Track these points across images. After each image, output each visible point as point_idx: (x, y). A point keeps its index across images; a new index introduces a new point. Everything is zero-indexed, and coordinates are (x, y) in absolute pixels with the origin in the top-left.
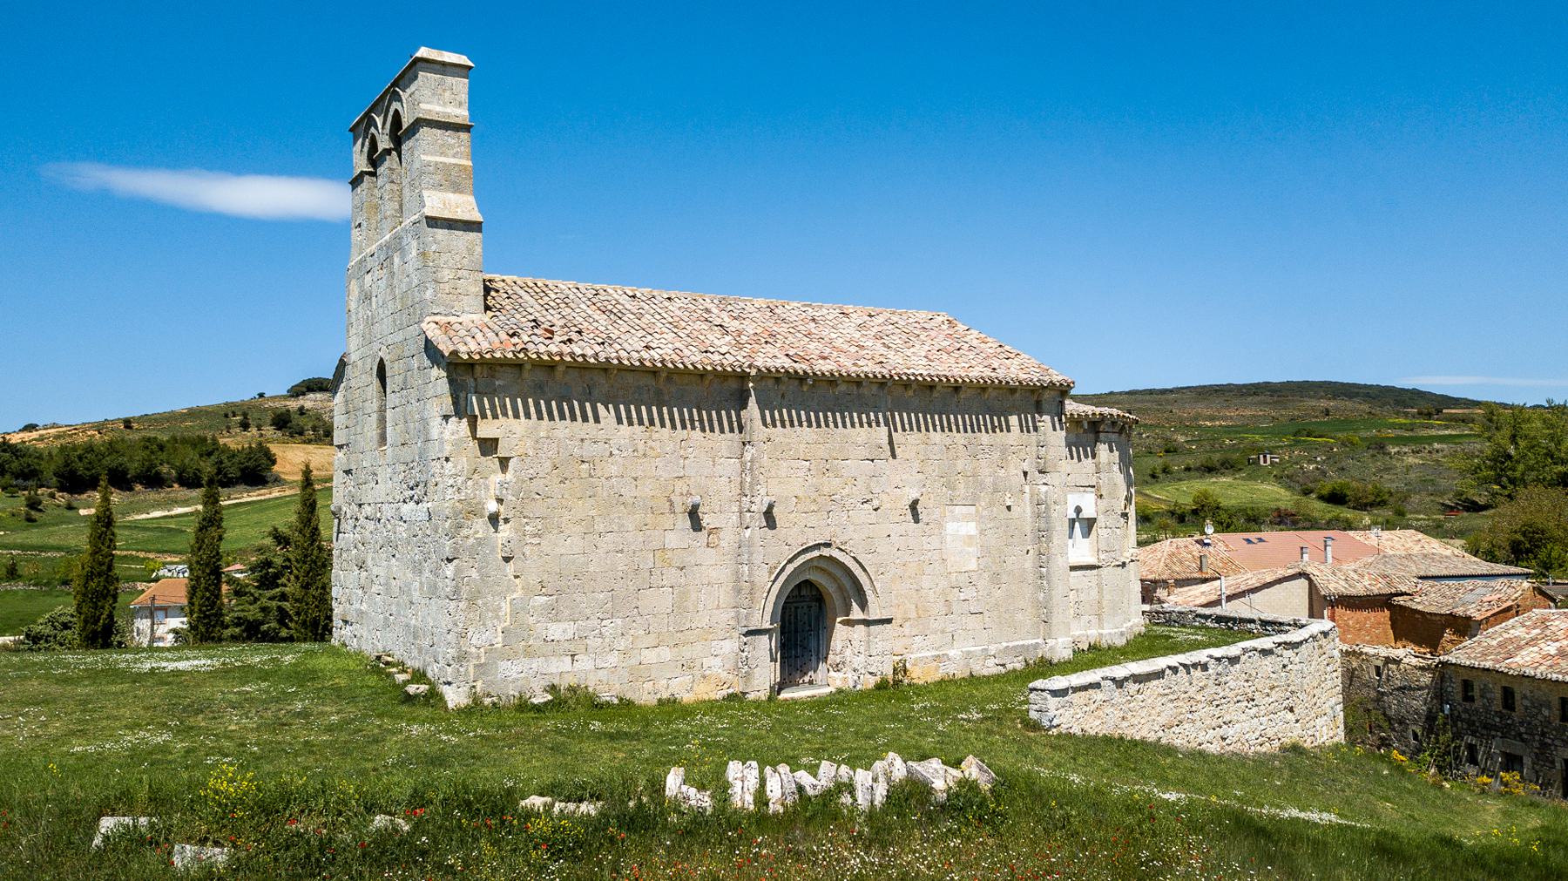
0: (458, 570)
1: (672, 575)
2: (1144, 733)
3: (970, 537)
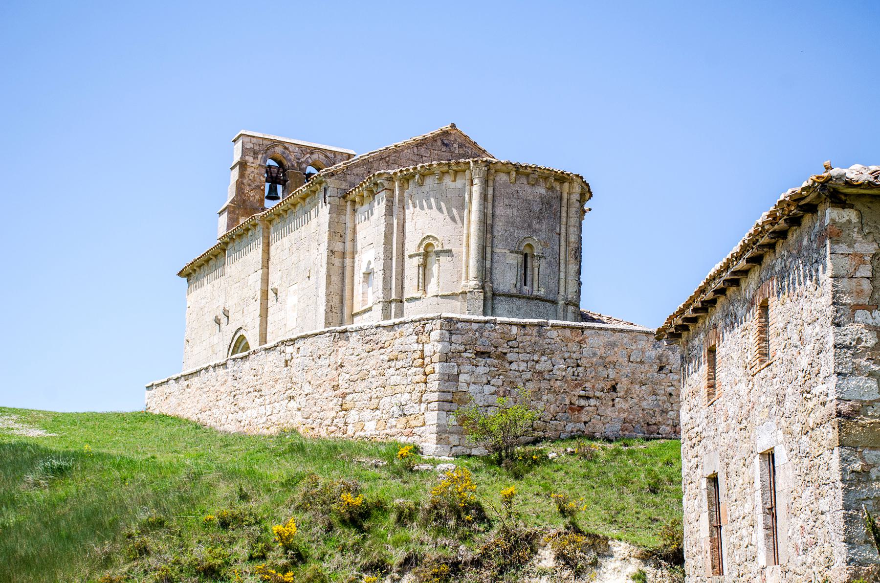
2: (189, 415)
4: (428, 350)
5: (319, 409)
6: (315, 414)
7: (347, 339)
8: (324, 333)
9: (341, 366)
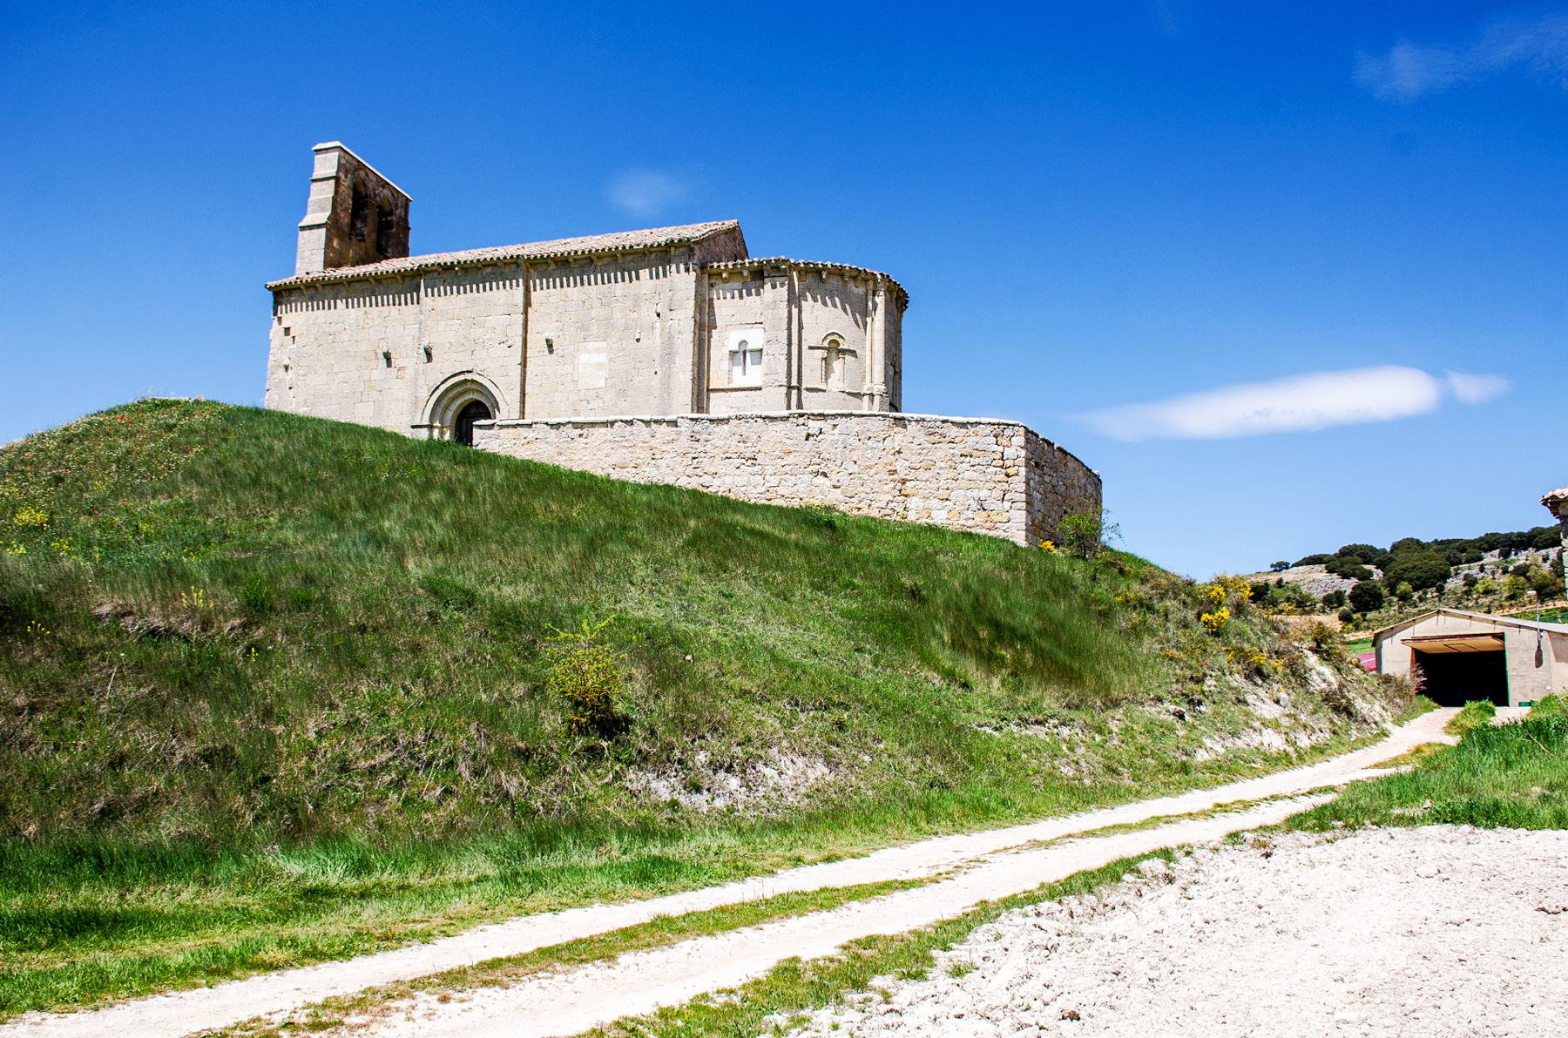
0: (270, 396)
1: (374, 395)
3: (601, 364)
4: (1008, 452)
5: (868, 490)
6: (863, 495)
7: (905, 427)
8: (876, 416)
9: (899, 452)
